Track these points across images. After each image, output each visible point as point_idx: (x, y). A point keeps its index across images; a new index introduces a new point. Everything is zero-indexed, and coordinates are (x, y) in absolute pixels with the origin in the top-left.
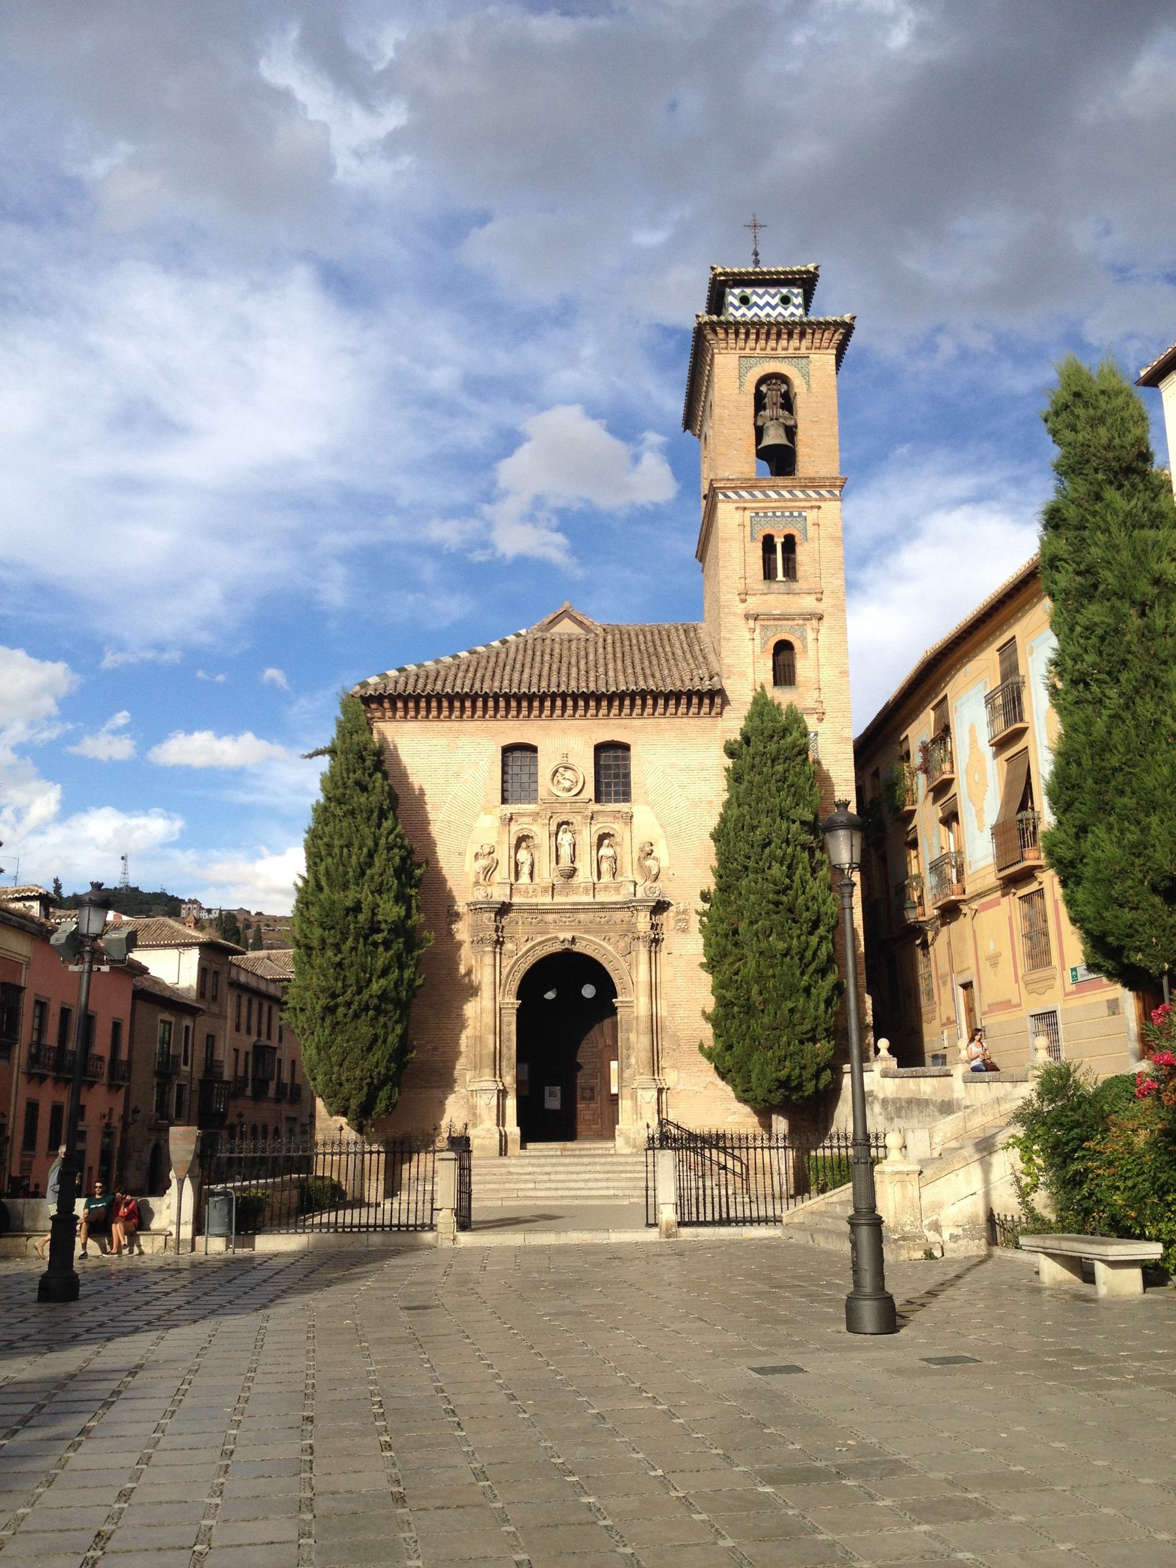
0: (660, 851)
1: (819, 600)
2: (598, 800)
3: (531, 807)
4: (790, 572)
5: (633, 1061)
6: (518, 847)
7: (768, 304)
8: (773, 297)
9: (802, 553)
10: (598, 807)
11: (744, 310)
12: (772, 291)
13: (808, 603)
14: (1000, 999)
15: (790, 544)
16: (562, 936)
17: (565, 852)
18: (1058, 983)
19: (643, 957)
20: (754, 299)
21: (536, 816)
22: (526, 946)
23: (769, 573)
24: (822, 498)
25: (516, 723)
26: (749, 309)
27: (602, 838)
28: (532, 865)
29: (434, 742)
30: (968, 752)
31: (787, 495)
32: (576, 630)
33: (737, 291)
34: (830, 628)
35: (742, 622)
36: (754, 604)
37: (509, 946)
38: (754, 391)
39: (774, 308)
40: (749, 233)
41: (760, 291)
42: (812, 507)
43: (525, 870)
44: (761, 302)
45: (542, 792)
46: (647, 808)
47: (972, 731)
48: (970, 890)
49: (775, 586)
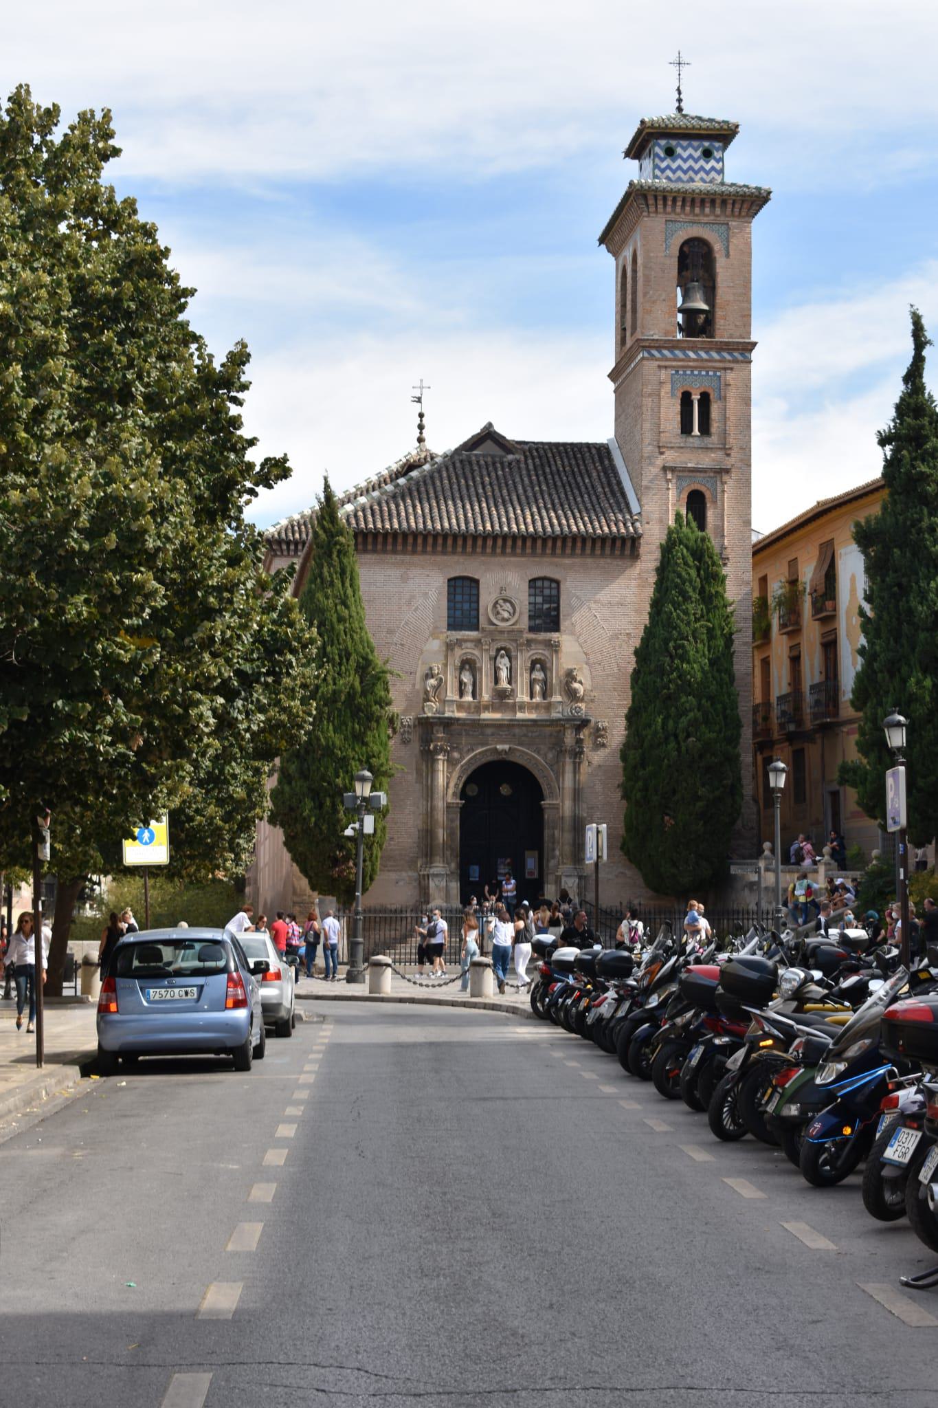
3: (473, 634)
4: (705, 429)
5: (557, 853)
6: (462, 669)
7: (690, 156)
8: (696, 150)
10: (532, 636)
11: (667, 162)
12: (695, 143)
15: (705, 400)
17: (504, 674)
19: (569, 768)
20: (679, 150)
21: (478, 642)
23: (686, 428)
24: (736, 361)
25: (461, 559)
26: (674, 161)
27: (534, 663)
29: (388, 572)
30: (848, 597)
32: (498, 451)
33: (663, 142)
36: (670, 457)
38: (677, 254)
39: (696, 161)
40: (675, 69)
41: (685, 143)
42: (725, 369)
44: (685, 155)
45: (482, 619)
47: (853, 579)
49: (691, 440)
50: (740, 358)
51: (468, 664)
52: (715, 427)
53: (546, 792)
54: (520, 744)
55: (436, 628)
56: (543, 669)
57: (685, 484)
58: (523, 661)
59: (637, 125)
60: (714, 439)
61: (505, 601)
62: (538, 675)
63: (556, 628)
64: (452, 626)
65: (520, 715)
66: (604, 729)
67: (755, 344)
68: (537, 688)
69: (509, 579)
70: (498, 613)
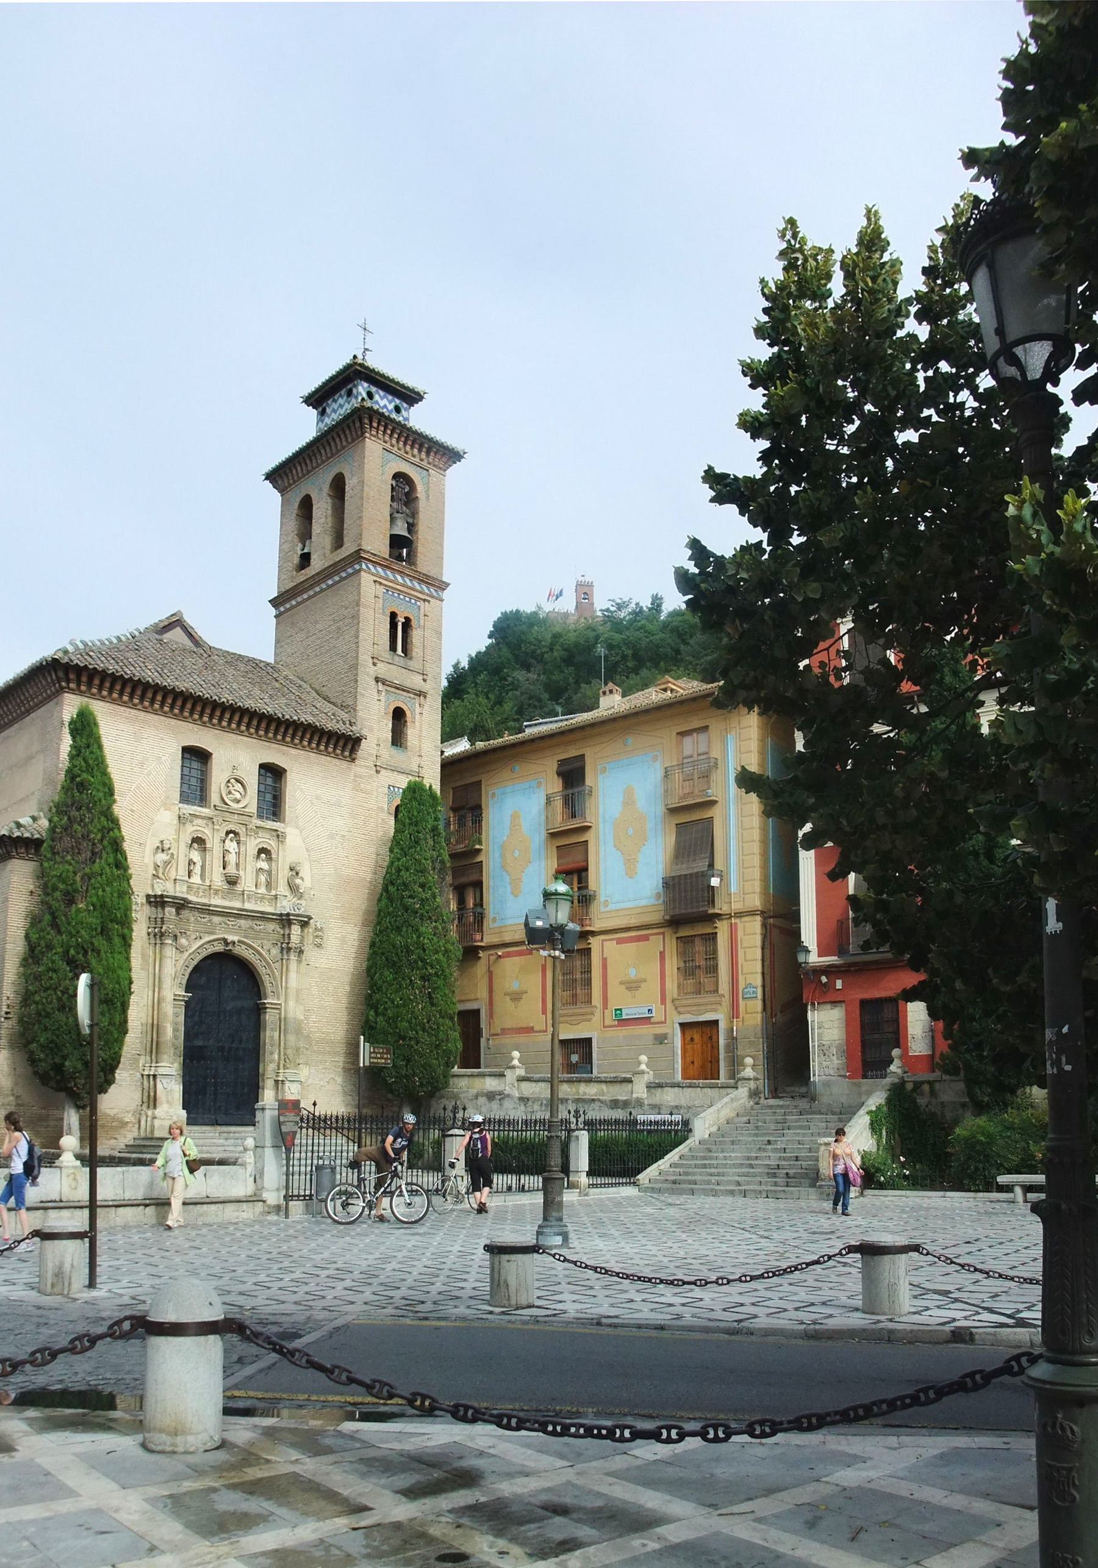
0: (305, 872)
1: (425, 680)
2: (260, 816)
3: (206, 811)
8: (390, 402)
9: (416, 635)
10: (259, 823)
12: (390, 397)
13: (416, 681)
14: (524, 1025)
16: (230, 938)
17: (232, 858)
18: (597, 1018)
20: (377, 397)
22: (197, 943)
23: (393, 648)
27: (262, 851)
28: (203, 867)
31: (409, 583)
33: (366, 385)
34: (430, 707)
35: (374, 683)
36: (382, 670)
37: (183, 941)
41: (382, 393)
42: (424, 600)
43: (197, 870)
45: (214, 799)
46: (297, 832)
48: (488, 939)
50: (435, 594)
51: (199, 841)
52: (416, 650)
53: (269, 988)
54: (245, 937)
55: (167, 797)
56: (269, 859)
57: (392, 699)
58: (252, 845)
59: (348, 360)
60: (414, 664)
61: (237, 781)
62: (265, 865)
63: (284, 822)
64: (185, 798)
65: (248, 906)
66: (321, 930)
67: (448, 585)
68: (263, 878)
69: (241, 759)
70: (230, 793)
